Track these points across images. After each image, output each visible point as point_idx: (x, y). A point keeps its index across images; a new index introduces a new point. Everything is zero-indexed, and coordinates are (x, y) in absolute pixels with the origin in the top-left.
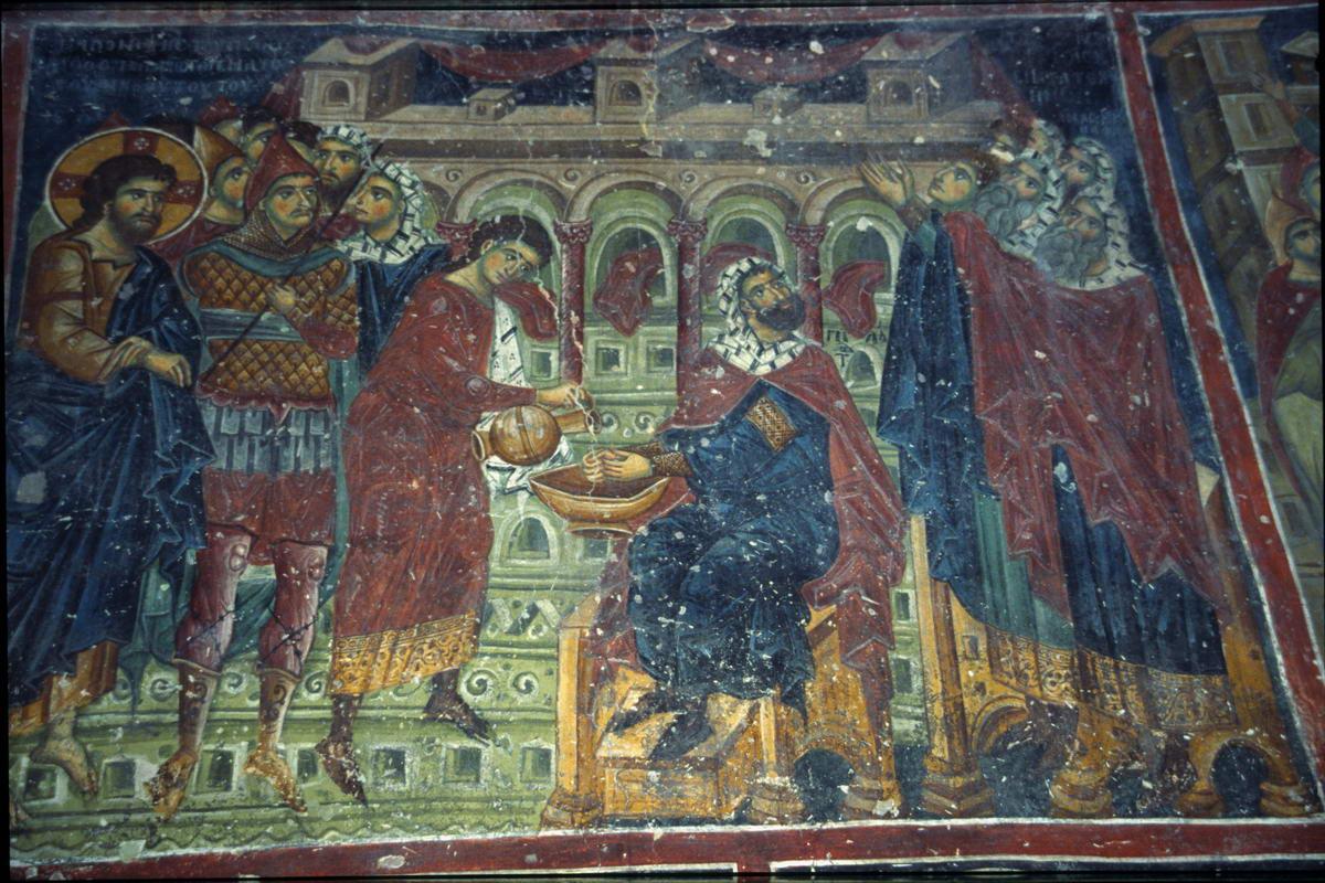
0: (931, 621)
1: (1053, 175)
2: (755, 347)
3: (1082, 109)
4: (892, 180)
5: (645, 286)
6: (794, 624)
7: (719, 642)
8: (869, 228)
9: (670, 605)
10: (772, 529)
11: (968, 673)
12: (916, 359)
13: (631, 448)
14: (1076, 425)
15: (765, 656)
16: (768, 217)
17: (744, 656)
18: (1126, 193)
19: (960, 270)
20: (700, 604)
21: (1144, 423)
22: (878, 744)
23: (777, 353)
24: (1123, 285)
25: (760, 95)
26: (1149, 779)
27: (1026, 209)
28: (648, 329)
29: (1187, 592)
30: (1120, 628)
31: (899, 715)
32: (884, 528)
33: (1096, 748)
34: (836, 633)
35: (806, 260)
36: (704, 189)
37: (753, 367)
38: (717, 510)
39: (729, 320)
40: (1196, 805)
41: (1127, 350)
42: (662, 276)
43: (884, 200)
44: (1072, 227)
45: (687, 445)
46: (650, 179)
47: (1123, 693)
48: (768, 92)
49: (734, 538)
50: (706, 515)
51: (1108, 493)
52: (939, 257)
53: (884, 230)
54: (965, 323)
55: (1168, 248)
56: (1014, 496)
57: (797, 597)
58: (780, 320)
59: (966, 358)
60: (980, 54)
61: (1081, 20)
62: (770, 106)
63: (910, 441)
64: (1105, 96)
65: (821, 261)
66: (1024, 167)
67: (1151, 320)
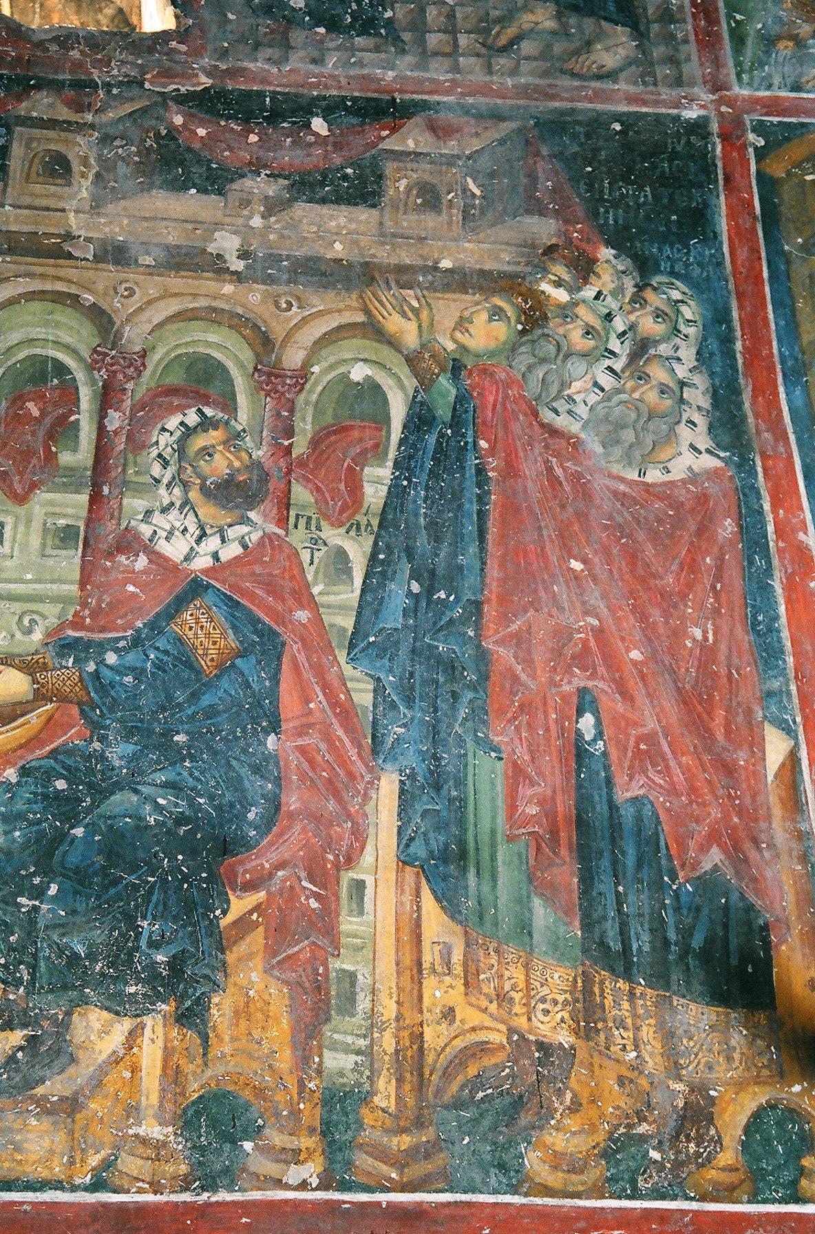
1: (619, 324)
2: (192, 528)
3: (664, 239)
4: (404, 314)
5: (51, 436)
7: (98, 936)
9: (37, 881)
11: (436, 992)
14: (612, 661)
15: (160, 958)
16: (232, 353)
17: (130, 955)
18: (712, 354)
20: (78, 880)
21: (703, 666)
23: (223, 541)
24: (694, 477)
25: (235, 186)
26: (659, 1148)
27: (576, 367)
29: (735, 896)
30: (642, 941)
31: (334, 1047)
32: (340, 785)
34: (261, 929)
35: (278, 414)
36: (152, 312)
37: (187, 558)
38: (119, 752)
39: (162, 491)
40: (716, 1184)
41: (692, 565)
42: (76, 425)
43: (392, 343)
44: (636, 395)
45: (87, 660)
46: (73, 290)
47: (637, 1029)
48: (248, 183)
49: (136, 791)
50: (102, 758)
51: (647, 755)
52: (456, 422)
53: (386, 382)
54: (482, 515)
55: (758, 432)
56: (522, 754)
58: (234, 494)
59: (478, 565)
60: (537, 154)
61: (677, 118)
62: (249, 202)
63: (391, 671)
64: (698, 222)
65: (298, 415)
66: (581, 311)
67: (728, 527)
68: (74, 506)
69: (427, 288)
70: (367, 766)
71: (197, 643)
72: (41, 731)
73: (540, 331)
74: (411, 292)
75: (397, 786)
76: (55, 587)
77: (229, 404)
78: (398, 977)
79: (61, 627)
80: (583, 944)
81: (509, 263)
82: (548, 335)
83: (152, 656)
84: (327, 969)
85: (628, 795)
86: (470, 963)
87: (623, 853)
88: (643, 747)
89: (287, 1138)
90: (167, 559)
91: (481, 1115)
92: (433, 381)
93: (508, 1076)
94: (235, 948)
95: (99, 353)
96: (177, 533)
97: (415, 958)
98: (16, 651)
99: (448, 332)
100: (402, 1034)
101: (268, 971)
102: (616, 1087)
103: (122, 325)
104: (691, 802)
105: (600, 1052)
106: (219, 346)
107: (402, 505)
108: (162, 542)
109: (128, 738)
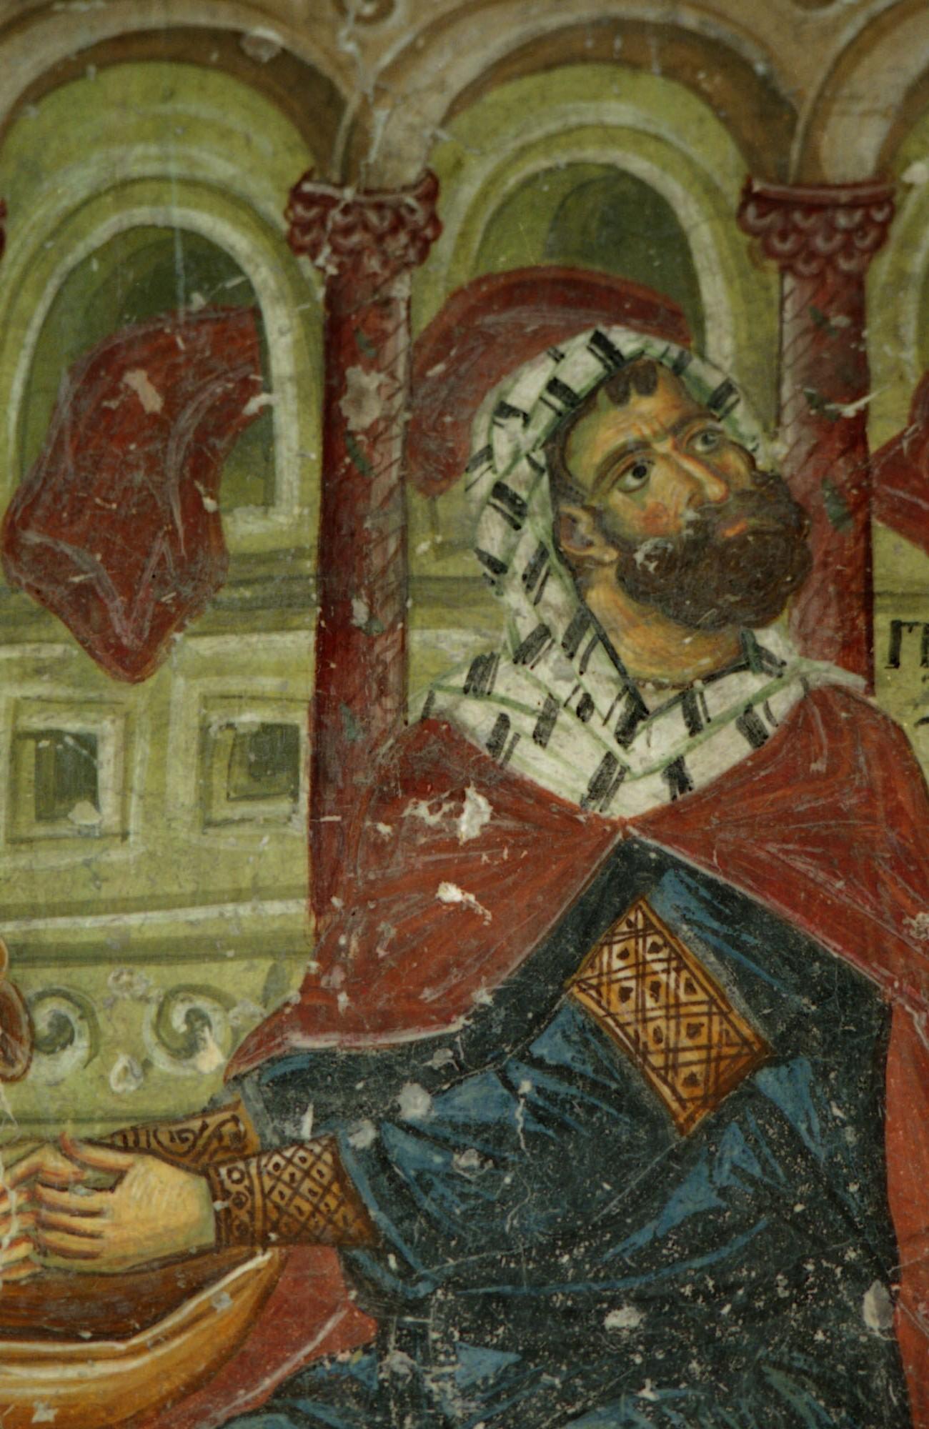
2: (606, 699)
5: (202, 465)
13: (137, 1138)
23: (694, 726)
28: (205, 646)
35: (818, 328)
37: (601, 787)
39: (515, 597)
50: (415, 1397)
58: (715, 583)
68: (280, 670)
71: (647, 1037)
72: (243, 1335)
76: (245, 910)
77: (676, 315)
79: (270, 1031)
83: (526, 1087)
90: (544, 798)
95: (310, 201)
96: (566, 718)
98: (161, 1105)
103: (366, 107)
106: (639, 137)
109: (479, 1330)
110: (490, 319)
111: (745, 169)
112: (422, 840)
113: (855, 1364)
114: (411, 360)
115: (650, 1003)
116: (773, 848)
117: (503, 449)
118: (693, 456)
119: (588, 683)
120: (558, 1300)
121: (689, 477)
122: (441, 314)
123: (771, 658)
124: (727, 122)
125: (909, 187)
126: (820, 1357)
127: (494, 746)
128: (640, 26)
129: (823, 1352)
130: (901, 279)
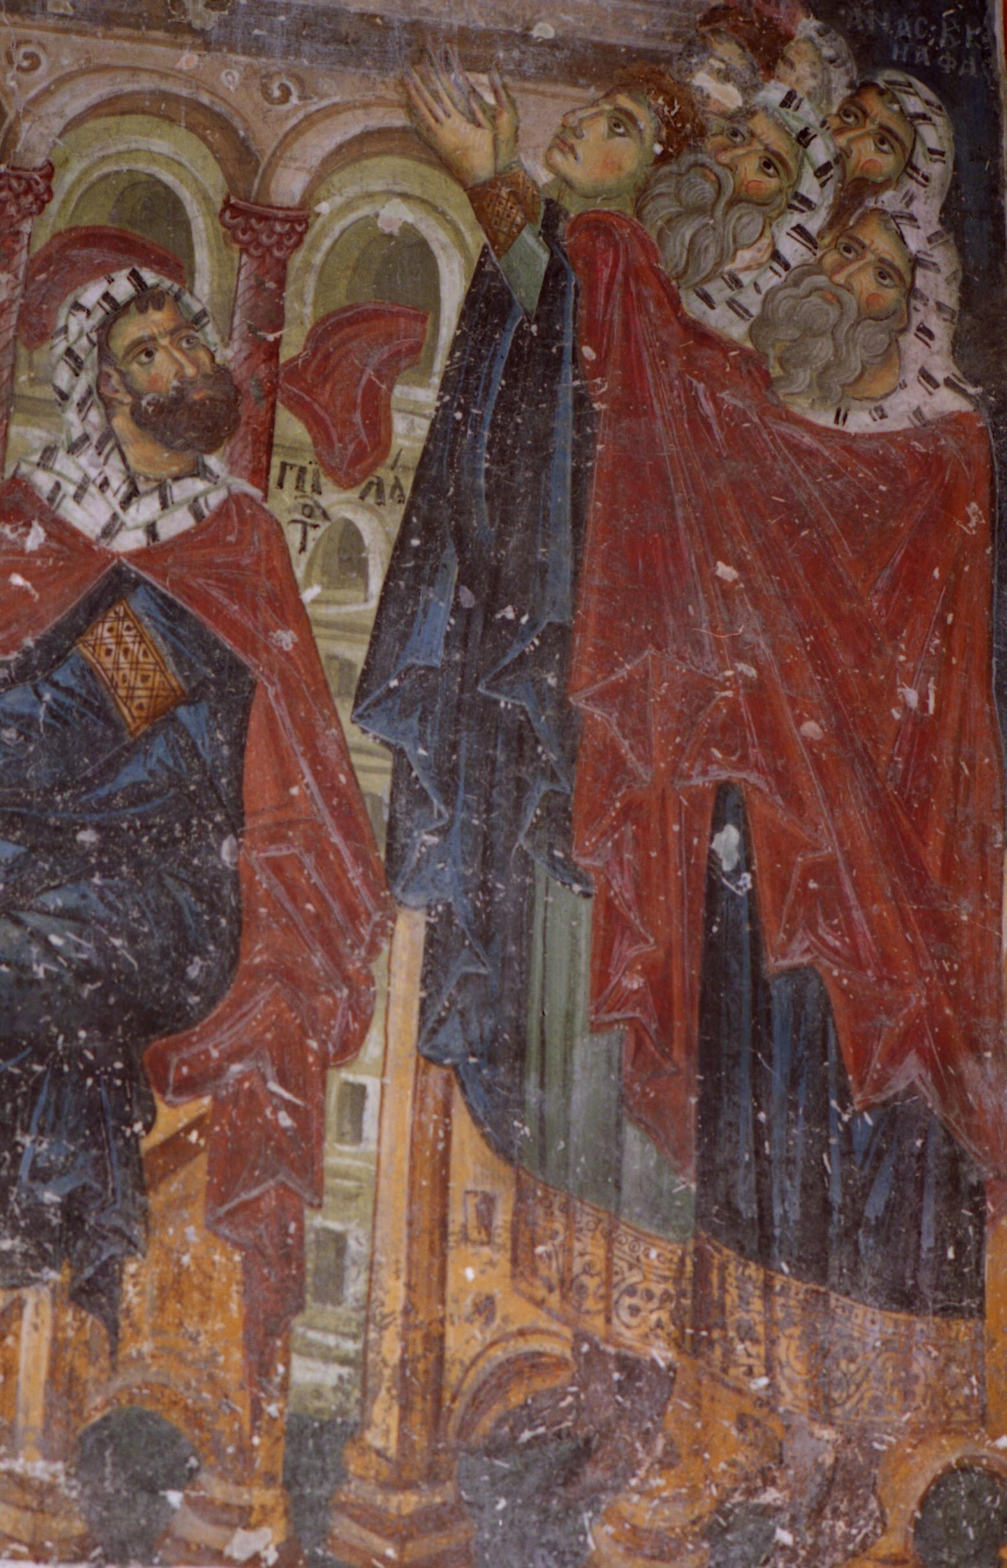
0: (404, 1150)
1: (820, 151)
2: (117, 481)
6: (118, 1132)
8: (408, 229)
10: (102, 912)
11: (468, 1273)
12: (461, 550)
14: (775, 740)
15: (49, 1196)
19: (588, 352)
22: (257, 1412)
23: (164, 505)
27: (750, 222)
31: (311, 1351)
33: (697, 1454)
34: (202, 1160)
37: (109, 532)
39: (72, 415)
43: (449, 165)
44: (840, 278)
47: (773, 1342)
49: (18, 922)
53: (437, 236)
57: (130, 1073)
59: (568, 564)
63: (421, 739)
66: (760, 124)
69: (511, 73)
70: (375, 895)
71: (118, 678)
73: (691, 158)
74: (484, 78)
75: (421, 932)
77: (179, 267)
78: (410, 1245)
80: (698, 1205)
81: (646, 35)
82: (703, 165)
83: (47, 697)
84: (301, 1228)
85: (785, 963)
86: (522, 1227)
87: (769, 1058)
88: (812, 885)
89: (232, 1488)
90: (75, 533)
91: (527, 1466)
92: (512, 237)
93: (570, 1407)
94: (162, 1187)
96: (93, 489)
97: (437, 1216)
99: (542, 151)
100: (411, 1335)
101: (212, 1226)
102: (734, 1432)
104: (880, 980)
105: (713, 1377)
106: (172, 162)
107: (451, 455)
108: (69, 504)
110: (74, 252)
111: (226, 189)
112: (4, 547)
113: (213, 880)
114: (27, 268)
115: (122, 659)
116: (201, 581)
117: (74, 329)
118: (180, 350)
119: (108, 471)
120: (52, 820)
121: (176, 361)
122: (48, 245)
123: (211, 473)
124: (219, 160)
125: (318, 215)
126: (194, 874)
127: (51, 500)
128: (177, 98)
129: (197, 870)
130: (308, 265)
